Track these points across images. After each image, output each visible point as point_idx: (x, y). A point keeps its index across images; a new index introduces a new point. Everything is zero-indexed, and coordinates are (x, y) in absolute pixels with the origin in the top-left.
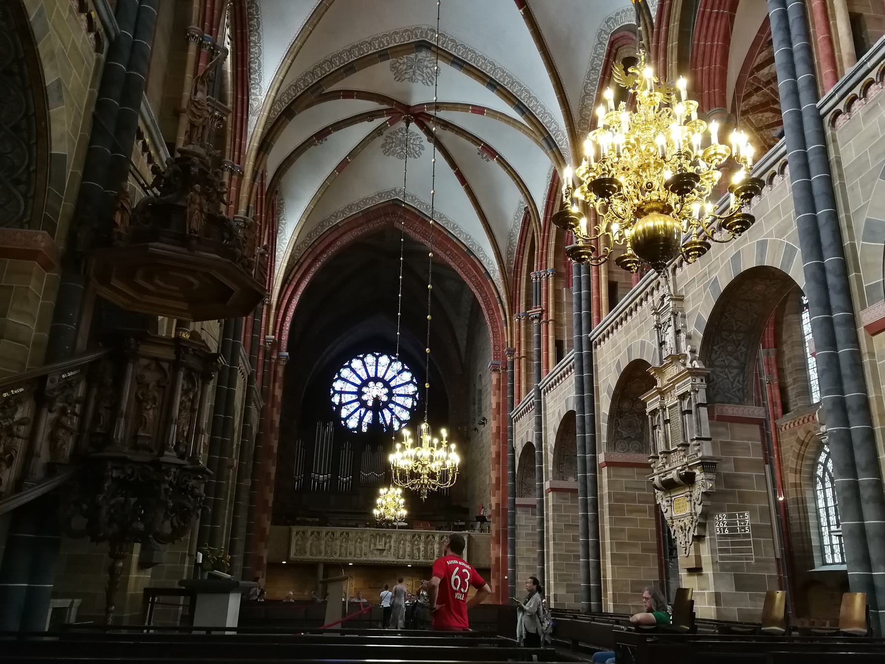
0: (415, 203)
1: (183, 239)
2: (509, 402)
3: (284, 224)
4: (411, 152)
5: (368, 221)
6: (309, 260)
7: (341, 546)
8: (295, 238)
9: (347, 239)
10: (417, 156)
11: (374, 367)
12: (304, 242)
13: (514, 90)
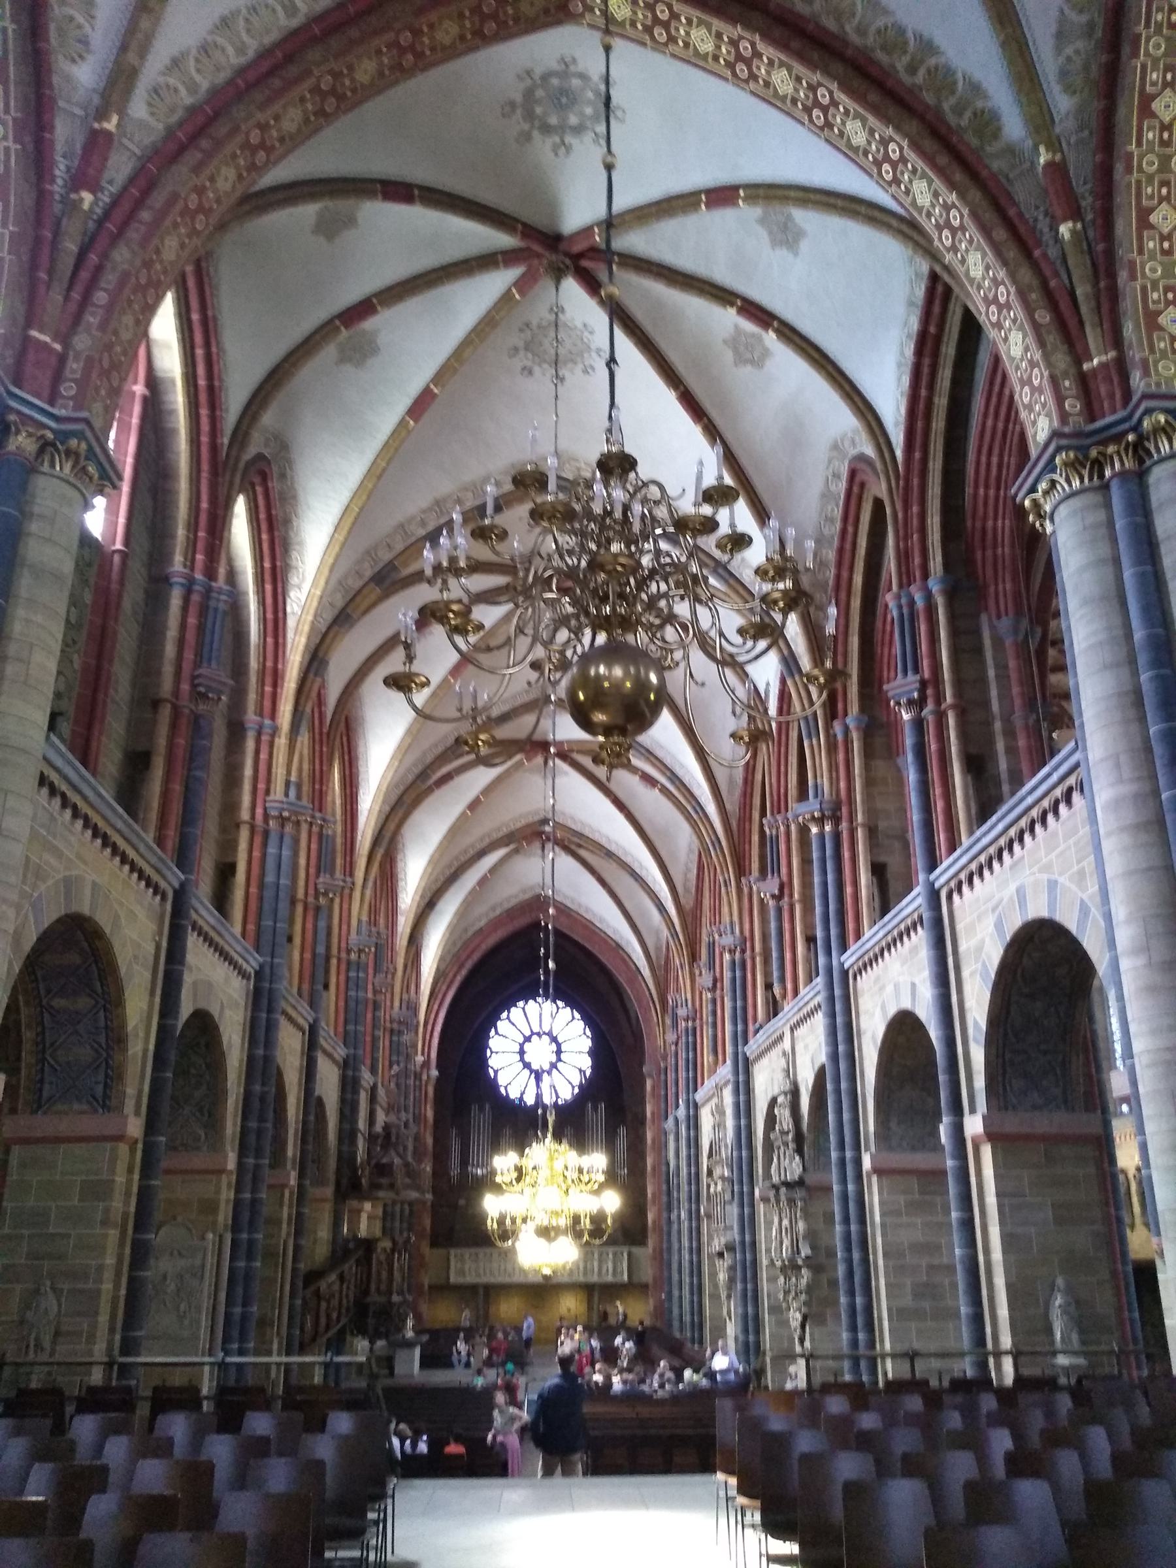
1: (392, 1186)
2: (663, 1112)
6: (455, 969)
9: (492, 941)
12: (449, 951)
13: (628, 860)
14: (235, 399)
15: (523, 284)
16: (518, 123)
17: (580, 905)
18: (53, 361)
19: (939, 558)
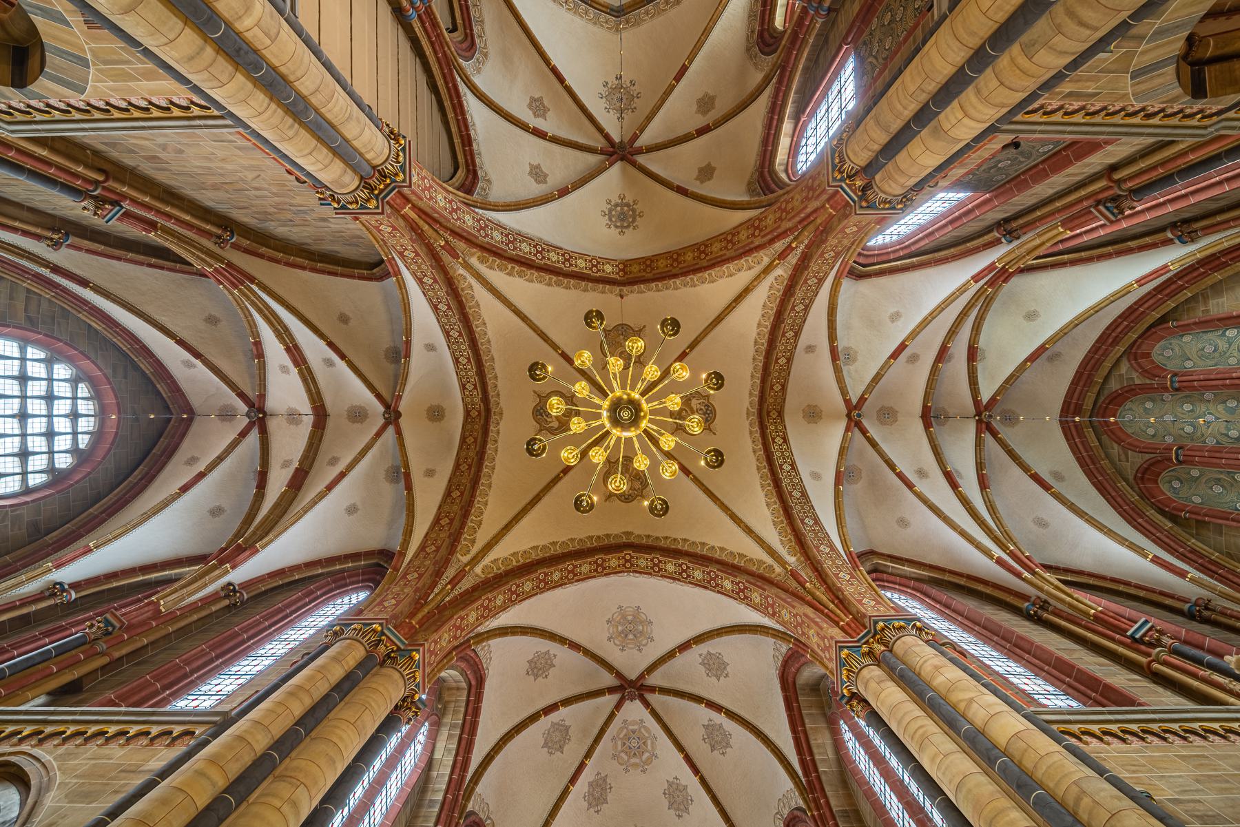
14: (763, 101)
15: (635, 137)
16: (638, 208)
18: (831, 202)
19: (416, 29)
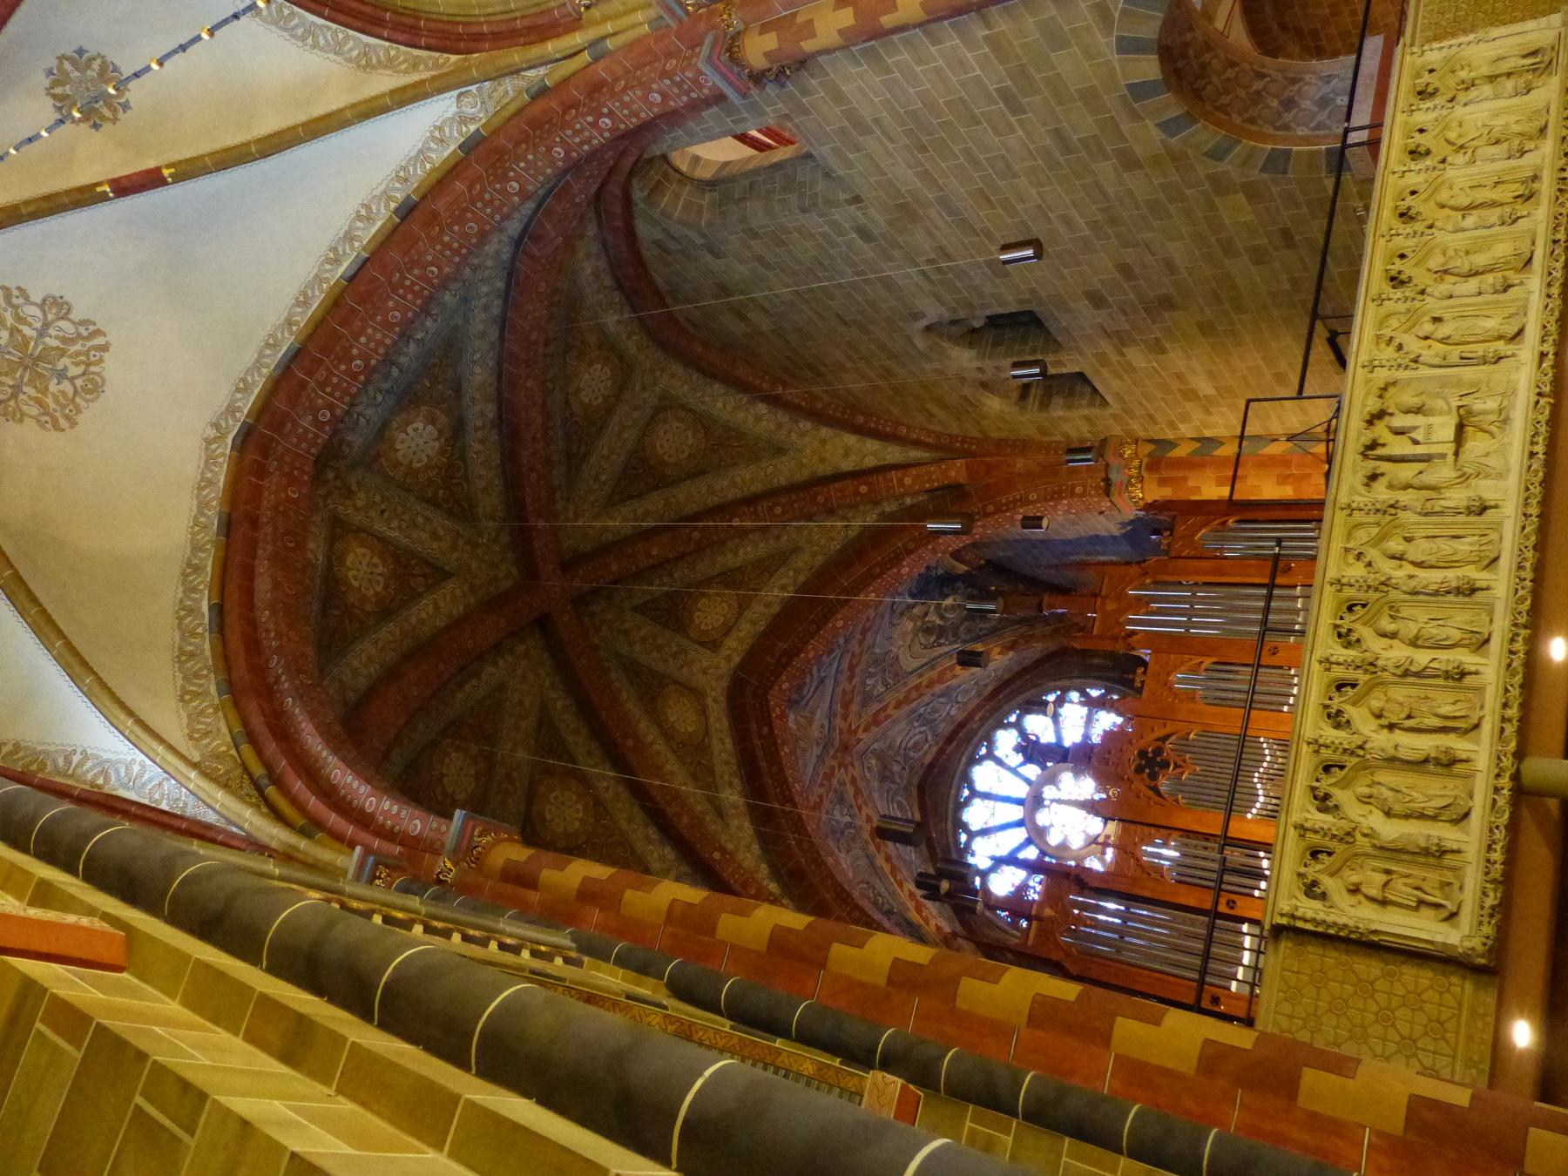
0: (254, 382)
3: (86, 756)
4: (78, 354)
5: (254, 523)
7: (1414, 643)
8: (130, 722)
10: (100, 341)
11: (999, 805)
17: (289, 323)
